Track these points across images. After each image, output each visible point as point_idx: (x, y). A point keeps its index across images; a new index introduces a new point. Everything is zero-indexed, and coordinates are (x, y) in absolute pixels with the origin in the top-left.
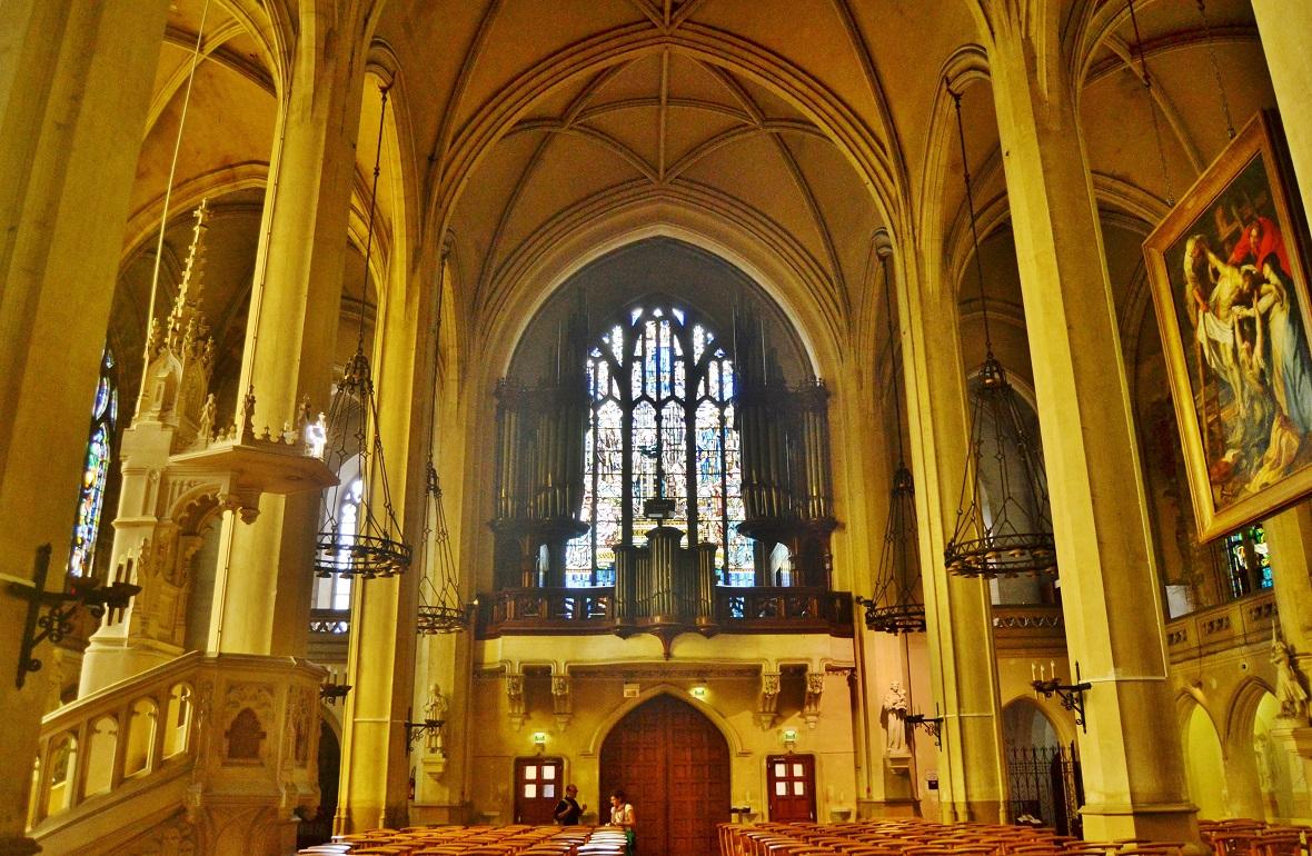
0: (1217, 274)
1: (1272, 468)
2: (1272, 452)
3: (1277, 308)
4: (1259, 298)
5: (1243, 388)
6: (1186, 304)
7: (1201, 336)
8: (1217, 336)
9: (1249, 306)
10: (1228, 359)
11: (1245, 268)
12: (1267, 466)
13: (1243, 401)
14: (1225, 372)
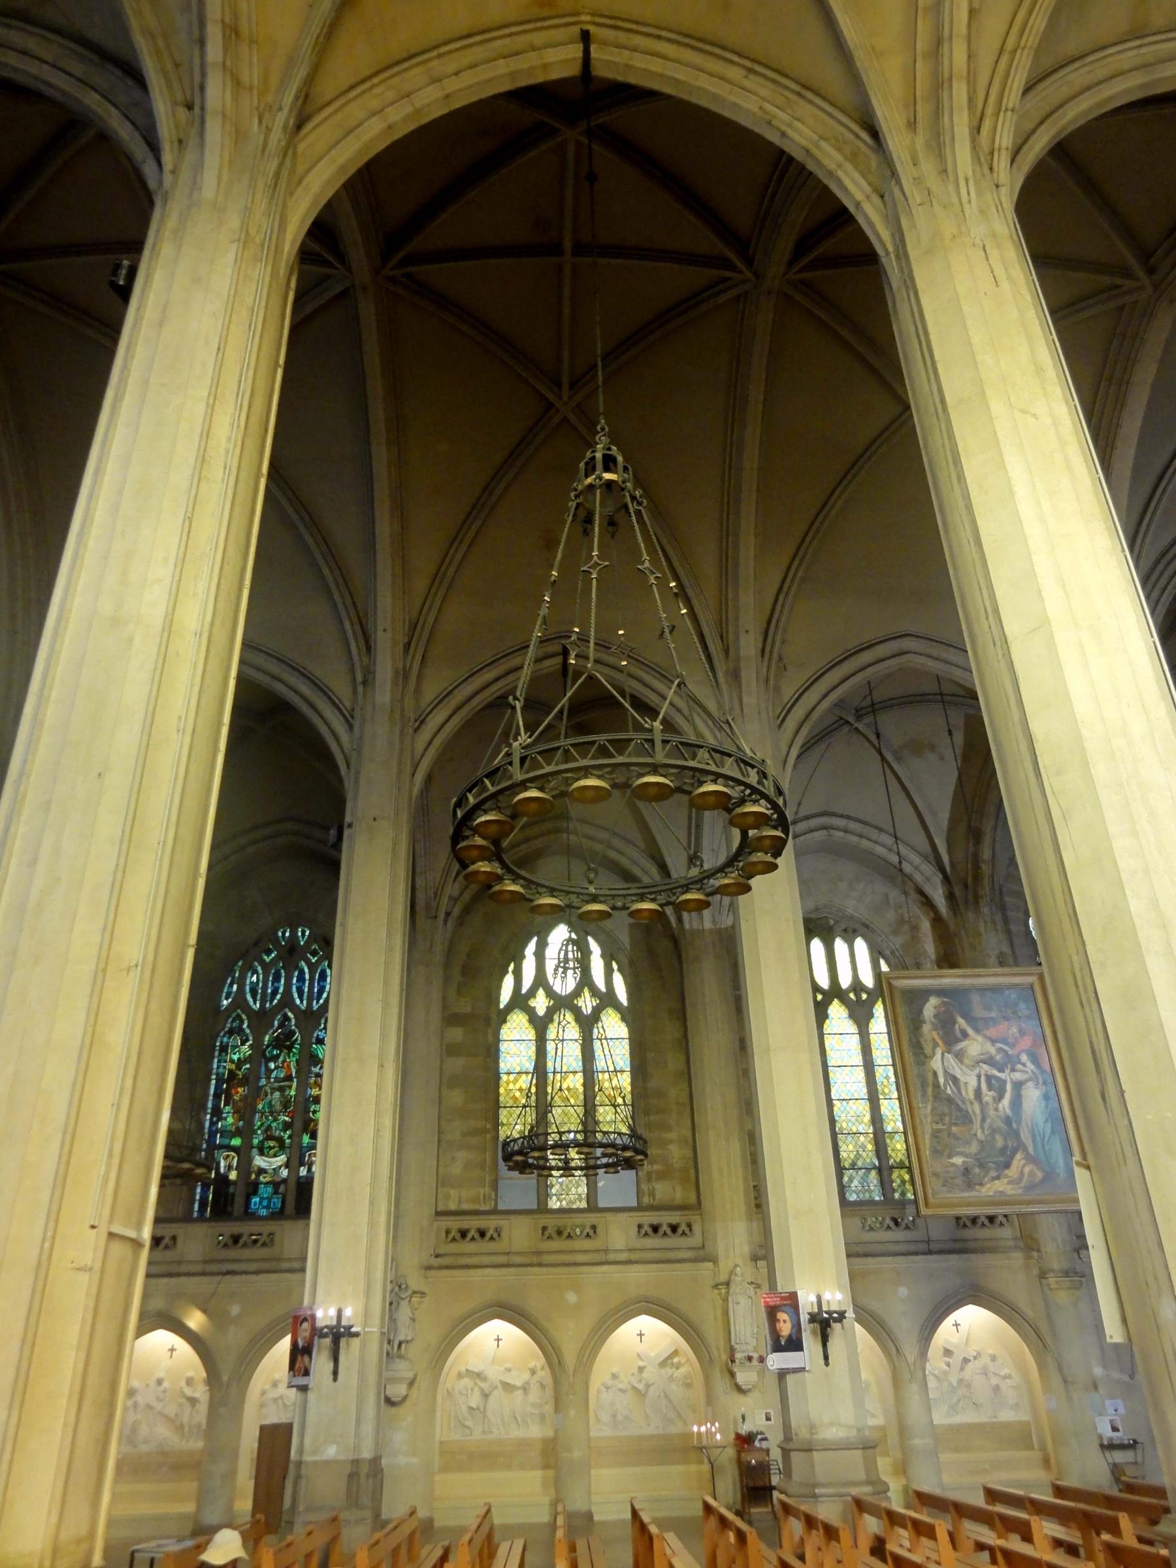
0: (965, 1035)
1: (1009, 1183)
2: (1013, 1172)
3: (1030, 1084)
4: (1013, 1070)
5: (983, 1120)
6: (921, 1035)
7: (936, 1063)
8: (958, 1073)
9: (1001, 1070)
10: (971, 1095)
11: (1000, 1045)
12: (1006, 1180)
13: (982, 1128)
14: (964, 1103)
